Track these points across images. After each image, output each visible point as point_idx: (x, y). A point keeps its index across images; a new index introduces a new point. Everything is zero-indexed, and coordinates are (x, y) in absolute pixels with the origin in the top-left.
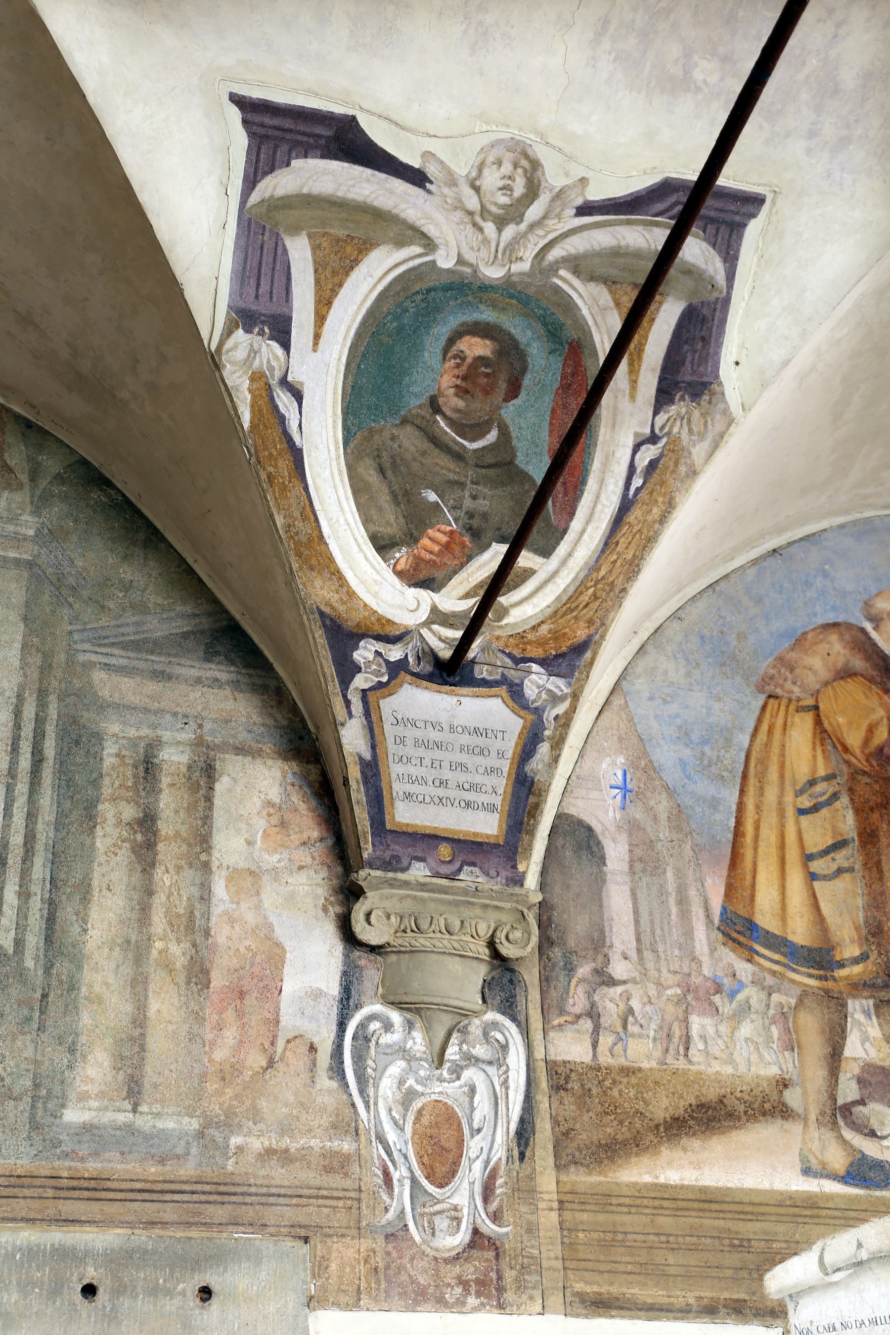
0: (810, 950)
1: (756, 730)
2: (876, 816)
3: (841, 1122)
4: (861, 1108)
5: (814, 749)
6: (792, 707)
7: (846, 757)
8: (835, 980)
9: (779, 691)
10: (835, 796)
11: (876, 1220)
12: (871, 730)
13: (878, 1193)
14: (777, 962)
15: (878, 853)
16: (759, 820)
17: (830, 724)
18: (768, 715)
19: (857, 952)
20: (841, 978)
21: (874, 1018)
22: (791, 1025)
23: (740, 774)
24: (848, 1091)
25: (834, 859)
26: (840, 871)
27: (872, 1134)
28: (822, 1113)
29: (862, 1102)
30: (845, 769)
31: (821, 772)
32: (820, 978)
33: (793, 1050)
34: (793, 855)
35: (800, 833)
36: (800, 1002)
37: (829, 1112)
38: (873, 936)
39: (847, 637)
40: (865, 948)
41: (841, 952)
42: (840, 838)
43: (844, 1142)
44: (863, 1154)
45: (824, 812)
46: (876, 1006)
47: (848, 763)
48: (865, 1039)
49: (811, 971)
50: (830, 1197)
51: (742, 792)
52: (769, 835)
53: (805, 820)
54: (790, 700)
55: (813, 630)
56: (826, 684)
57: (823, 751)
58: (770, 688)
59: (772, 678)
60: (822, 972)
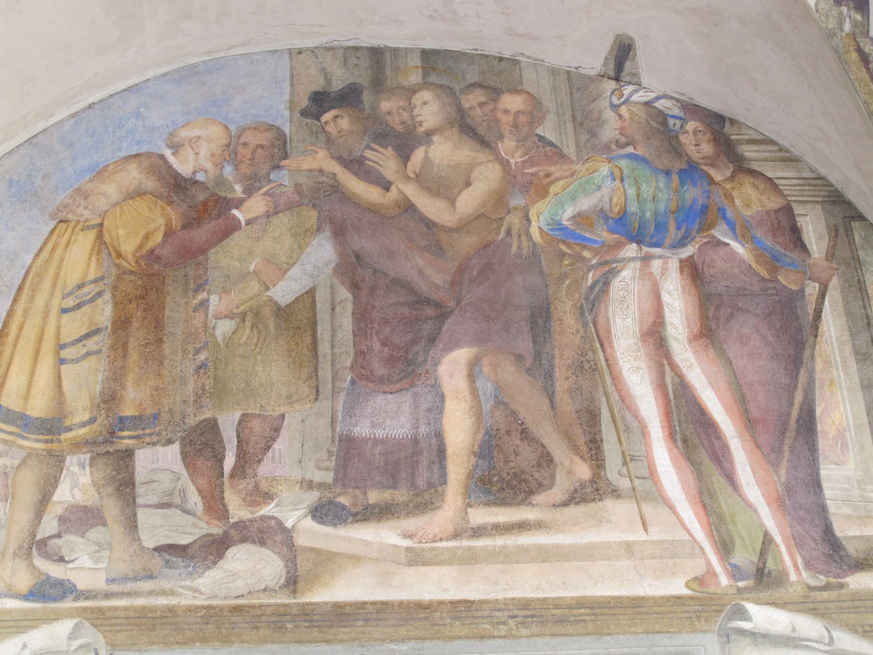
0: (44, 420)
1: (41, 250)
2: (134, 305)
3: (35, 552)
4: (56, 540)
5: (90, 259)
6: (79, 227)
7: (117, 261)
8: (59, 441)
9: (70, 216)
10: (99, 294)
11: (45, 626)
12: (147, 237)
13: (53, 605)
14: (11, 433)
15: (127, 336)
16: (24, 323)
17: (111, 237)
18: (55, 237)
19: (86, 417)
20: (66, 440)
21: (88, 469)
22: (10, 481)
23: (17, 287)
24: (49, 526)
25: (84, 345)
26: (88, 354)
27: (62, 559)
28: (20, 548)
29: (59, 536)
30: (114, 271)
31: (92, 276)
32: (46, 442)
33: (7, 501)
34: (48, 345)
35: (58, 328)
36: (24, 462)
37: (26, 546)
38: (105, 402)
39: (146, 164)
40: (95, 413)
41: (71, 420)
42: (94, 328)
43: (33, 567)
44: (48, 576)
45: (86, 309)
46: (92, 459)
47: (118, 266)
48: (75, 484)
49: (41, 437)
50: (10, 612)
51: (15, 301)
52: (30, 333)
53: (65, 317)
54: (78, 222)
55: (115, 162)
56: (116, 204)
57: (98, 260)
58: (62, 215)
59: (66, 206)
60: (49, 437)
